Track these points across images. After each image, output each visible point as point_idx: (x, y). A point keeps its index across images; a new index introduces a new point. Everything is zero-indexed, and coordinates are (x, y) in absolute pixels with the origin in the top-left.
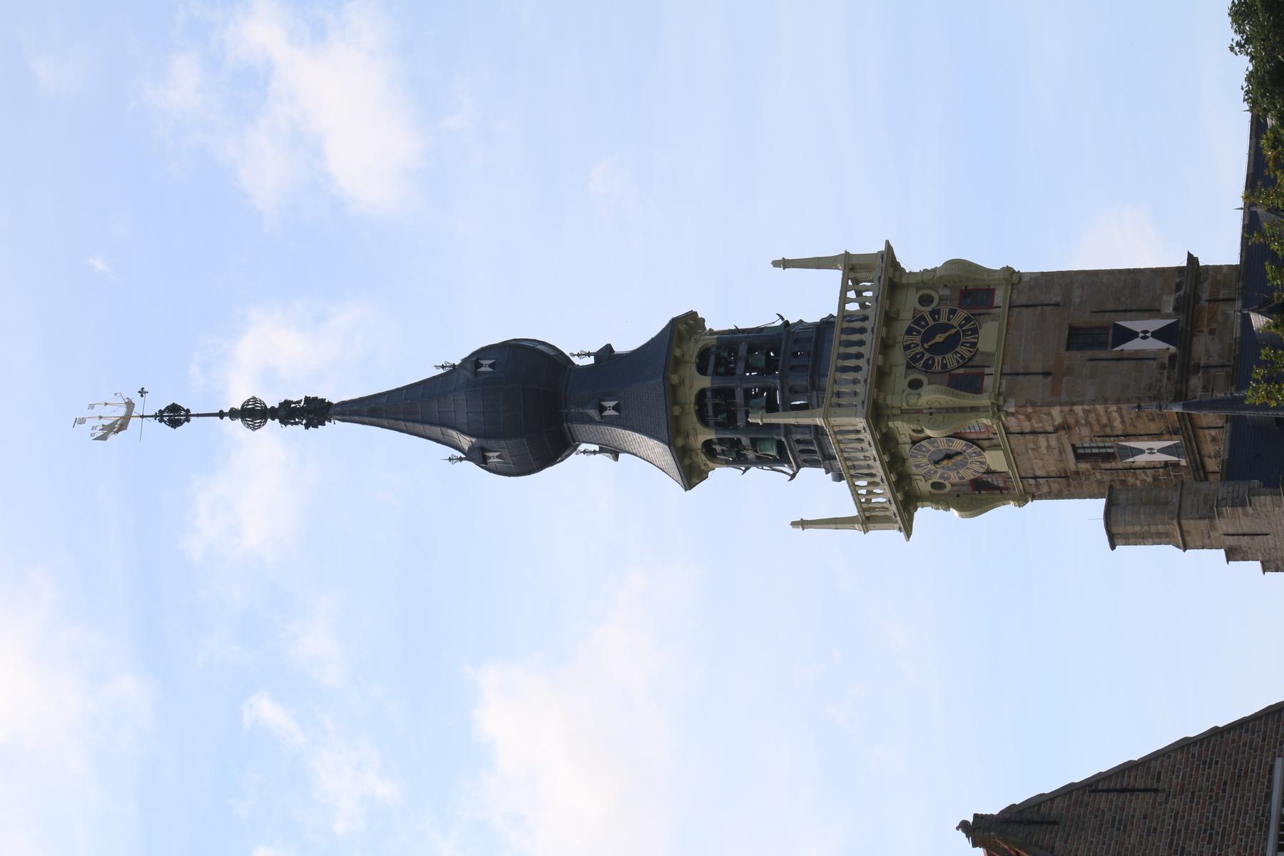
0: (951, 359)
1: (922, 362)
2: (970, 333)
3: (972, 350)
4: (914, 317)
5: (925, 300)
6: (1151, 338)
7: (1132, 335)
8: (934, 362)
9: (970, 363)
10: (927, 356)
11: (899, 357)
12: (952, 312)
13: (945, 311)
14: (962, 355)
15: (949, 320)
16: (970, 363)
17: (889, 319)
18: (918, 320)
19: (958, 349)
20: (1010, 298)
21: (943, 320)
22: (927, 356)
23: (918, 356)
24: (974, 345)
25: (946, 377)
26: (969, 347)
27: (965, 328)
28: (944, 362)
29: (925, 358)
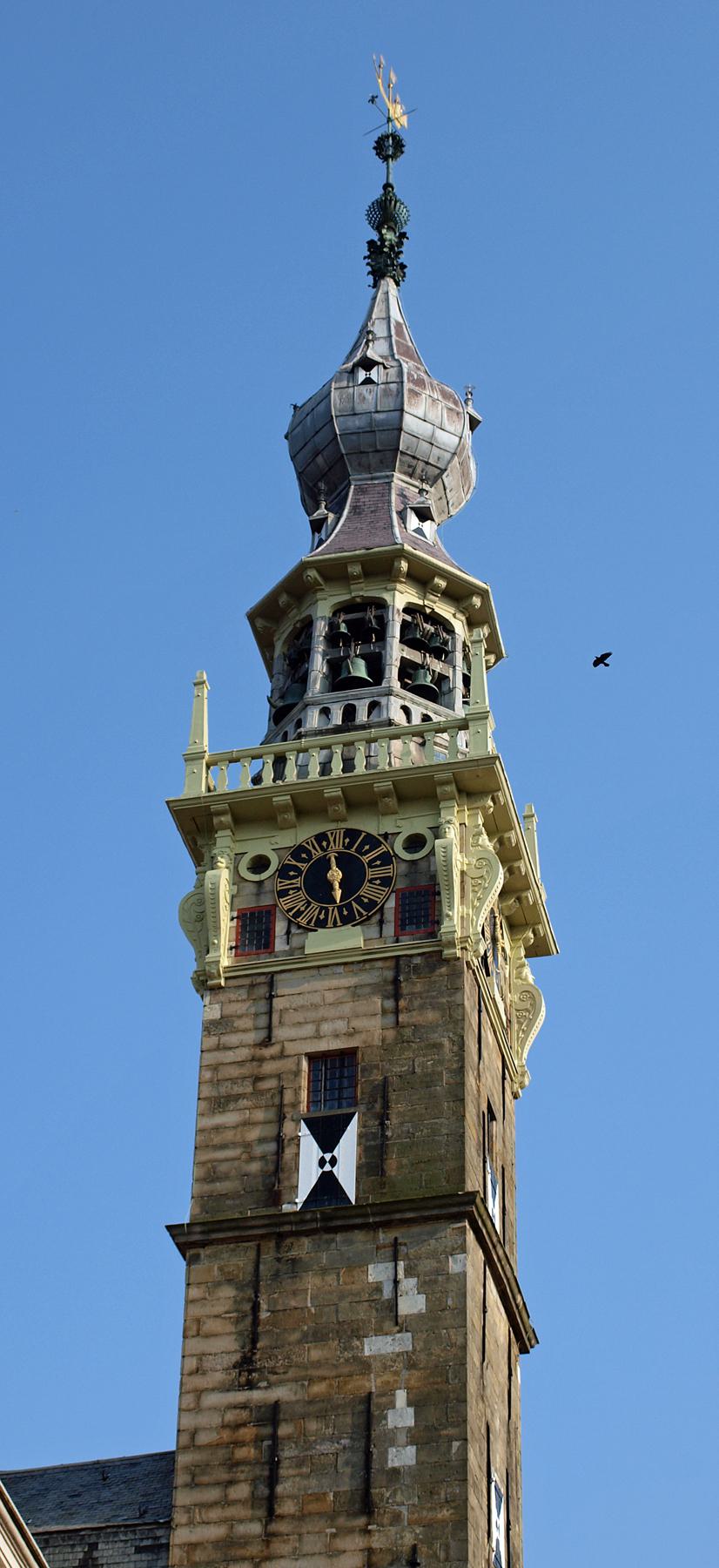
0: (297, 900)
1: (294, 863)
2: (345, 913)
3: (312, 924)
4: (386, 836)
5: (415, 842)
6: (320, 1171)
7: (328, 1136)
8: (294, 877)
9: (294, 930)
10: (304, 867)
11: (304, 834)
12: (386, 882)
13: (388, 871)
14: (303, 912)
15: (370, 881)
16: (294, 930)
17: (360, 798)
18: (372, 841)
19: (314, 905)
20: (411, 956)
21: (370, 874)
22: (304, 867)
23: (304, 856)
24: (322, 924)
25: (267, 901)
26: (318, 917)
27: (354, 905)
28: (291, 892)
29: (299, 864)
